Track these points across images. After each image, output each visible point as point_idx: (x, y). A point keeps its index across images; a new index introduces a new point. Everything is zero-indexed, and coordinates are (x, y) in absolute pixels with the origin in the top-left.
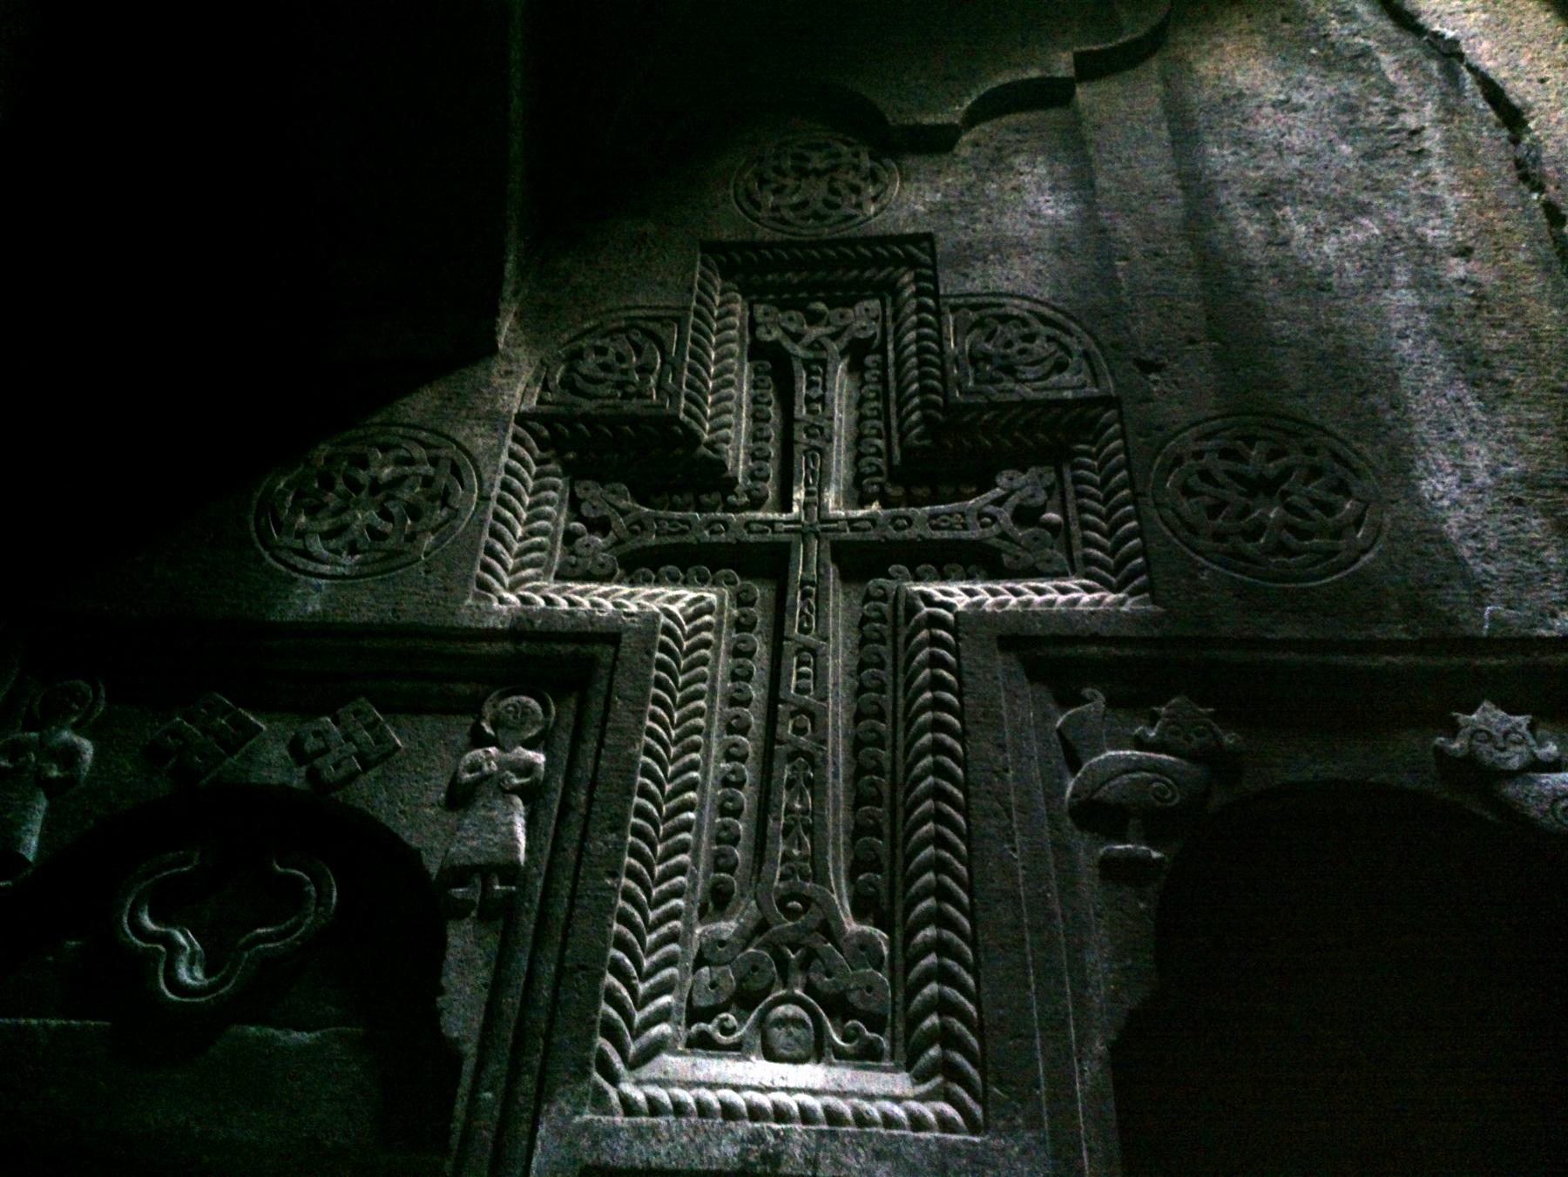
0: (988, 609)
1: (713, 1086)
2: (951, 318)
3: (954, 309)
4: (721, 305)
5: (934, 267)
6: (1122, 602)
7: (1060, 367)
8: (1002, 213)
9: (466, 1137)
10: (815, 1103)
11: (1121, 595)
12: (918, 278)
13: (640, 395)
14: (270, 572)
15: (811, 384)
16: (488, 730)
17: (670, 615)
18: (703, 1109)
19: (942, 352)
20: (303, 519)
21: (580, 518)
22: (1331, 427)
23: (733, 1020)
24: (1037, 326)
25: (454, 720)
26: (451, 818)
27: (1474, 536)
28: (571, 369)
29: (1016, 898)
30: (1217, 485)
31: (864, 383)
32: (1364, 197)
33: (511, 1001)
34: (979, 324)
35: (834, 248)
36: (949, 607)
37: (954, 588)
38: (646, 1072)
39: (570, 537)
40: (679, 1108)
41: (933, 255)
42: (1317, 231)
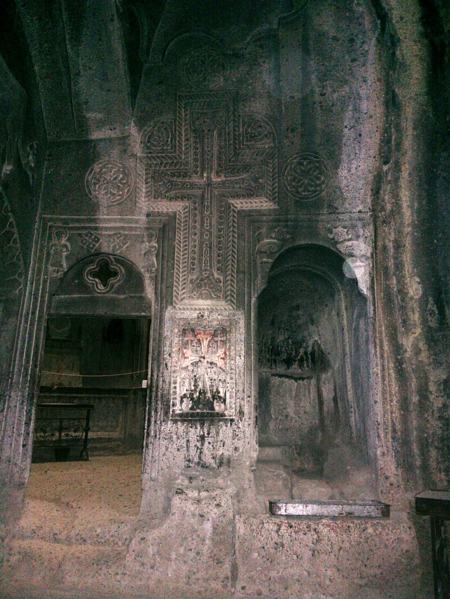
0: (244, 208)
1: (192, 305)
8: (256, 83)
10: (209, 307)
11: (272, 204)
17: (179, 211)
18: (192, 309)
23: (195, 293)
27: (348, 187)
29: (244, 272)
33: (159, 291)
36: (236, 208)
37: (238, 201)
40: (188, 309)
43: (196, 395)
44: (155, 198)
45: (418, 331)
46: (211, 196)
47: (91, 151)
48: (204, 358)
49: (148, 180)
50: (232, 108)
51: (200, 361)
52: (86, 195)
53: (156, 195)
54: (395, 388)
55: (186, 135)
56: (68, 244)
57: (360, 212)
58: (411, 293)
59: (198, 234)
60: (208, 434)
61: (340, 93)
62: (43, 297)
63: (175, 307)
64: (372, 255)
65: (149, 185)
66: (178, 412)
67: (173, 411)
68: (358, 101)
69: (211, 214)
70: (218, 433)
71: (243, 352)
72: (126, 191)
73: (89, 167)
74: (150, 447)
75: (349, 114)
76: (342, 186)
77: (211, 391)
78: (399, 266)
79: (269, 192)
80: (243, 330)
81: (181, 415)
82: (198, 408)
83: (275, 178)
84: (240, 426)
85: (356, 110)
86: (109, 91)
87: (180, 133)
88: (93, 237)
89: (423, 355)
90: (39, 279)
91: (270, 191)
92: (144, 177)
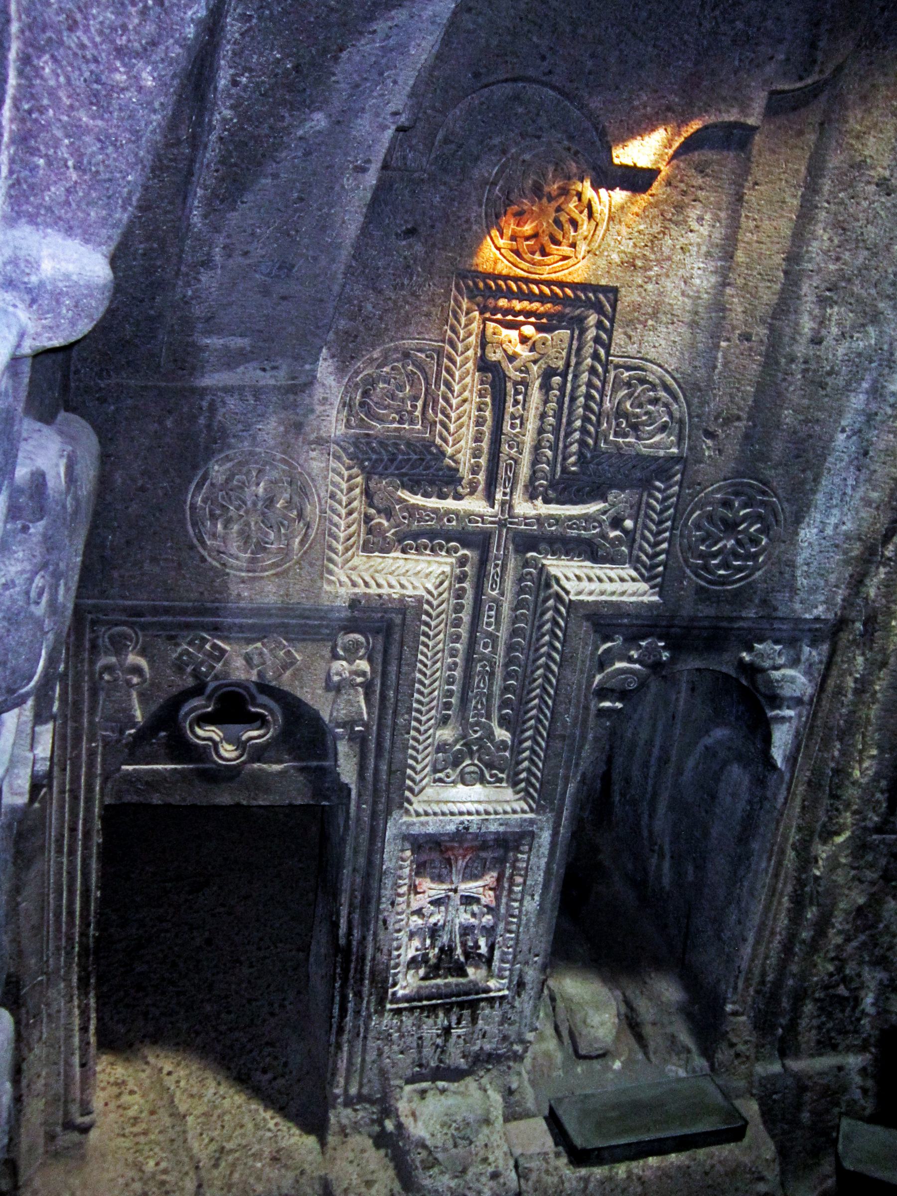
1: (446, 802)
2: (612, 374)
3: (617, 367)
4: (466, 326)
5: (612, 321)
6: (644, 594)
7: (664, 428)
9: (358, 819)
12: (599, 325)
13: (412, 422)
14: (213, 568)
15: (516, 402)
16: (341, 653)
17: (429, 592)
18: (443, 814)
19: (601, 404)
20: (219, 526)
21: (371, 505)
22: (780, 491)
24: (662, 394)
25: (320, 644)
26: (331, 695)
27: (808, 564)
28: (366, 393)
30: (715, 525)
31: (546, 402)
32: (881, 305)
33: (369, 774)
34: (629, 385)
35: (548, 286)
36: (567, 593)
38: (422, 797)
39: (368, 518)
40: (435, 814)
41: (614, 307)
42: (843, 334)
43: (433, 953)
44: (367, 548)
45: (848, 834)
46: (506, 548)
47: (202, 421)
48: (455, 891)
49: (355, 504)
50: (591, 333)
51: (448, 897)
52: (192, 547)
53: (374, 543)
54: (783, 921)
55: (464, 389)
56: (143, 663)
57: (817, 619)
58: (857, 773)
59: (465, 635)
60: (459, 1023)
61: (854, 345)
62: (90, 788)
63: (407, 812)
64: (811, 700)
65: (355, 515)
66: (400, 993)
67: (394, 994)
68: (886, 371)
69: (502, 594)
70: (474, 1020)
71: (539, 890)
72: (297, 540)
73: (195, 467)
74: (345, 1048)
75: (857, 401)
76: (800, 560)
77: (464, 944)
78: (852, 725)
79: (644, 558)
80: (545, 850)
81: (407, 999)
82: (437, 976)
83: (665, 531)
84: (517, 1004)
85: (876, 392)
86: (284, 298)
87: (448, 385)
88: (208, 647)
89: (839, 871)
90: (79, 756)
91: (647, 555)
92: (344, 500)
